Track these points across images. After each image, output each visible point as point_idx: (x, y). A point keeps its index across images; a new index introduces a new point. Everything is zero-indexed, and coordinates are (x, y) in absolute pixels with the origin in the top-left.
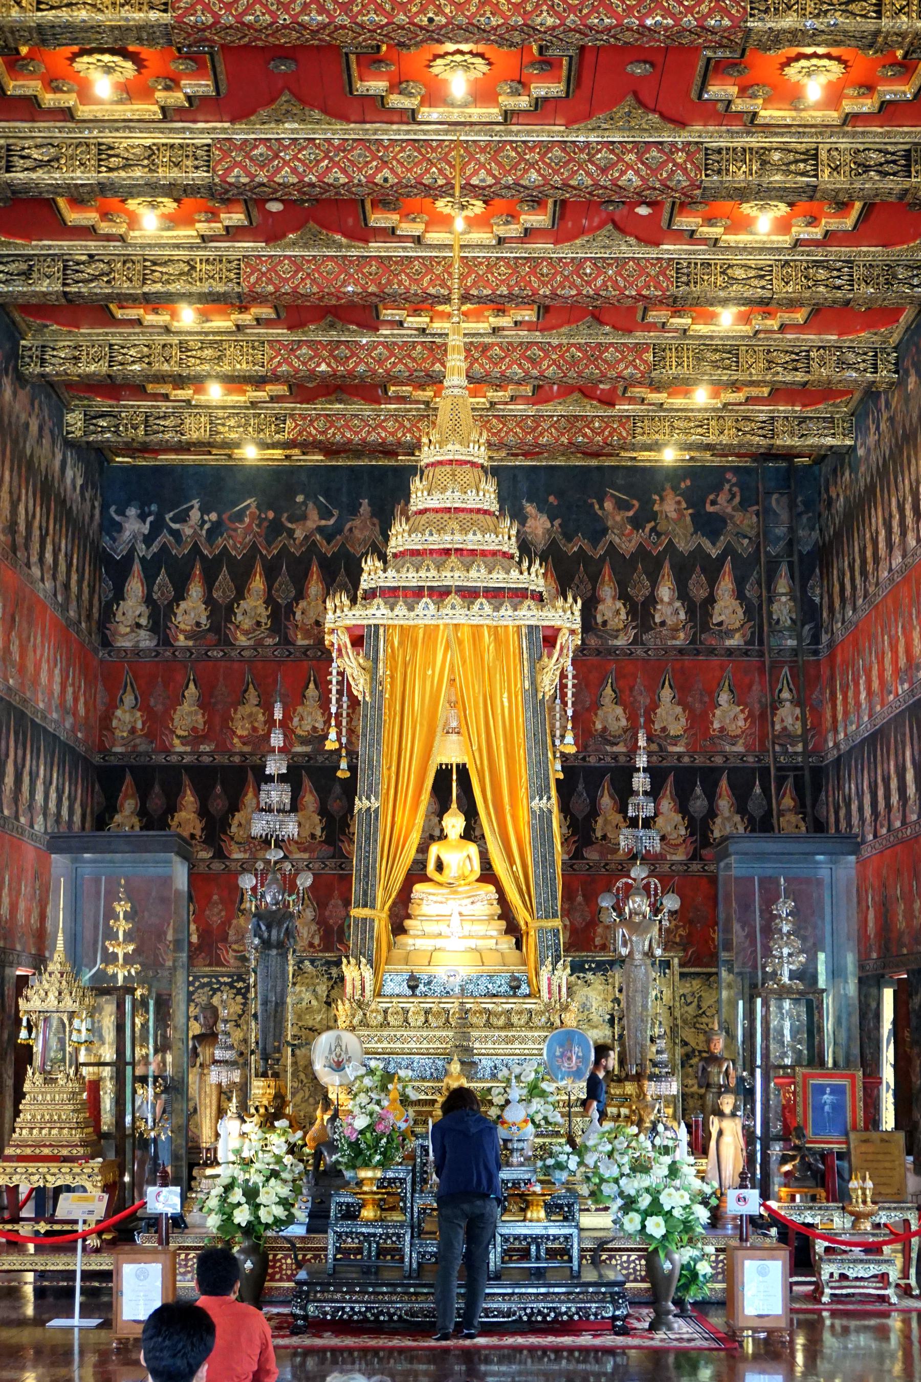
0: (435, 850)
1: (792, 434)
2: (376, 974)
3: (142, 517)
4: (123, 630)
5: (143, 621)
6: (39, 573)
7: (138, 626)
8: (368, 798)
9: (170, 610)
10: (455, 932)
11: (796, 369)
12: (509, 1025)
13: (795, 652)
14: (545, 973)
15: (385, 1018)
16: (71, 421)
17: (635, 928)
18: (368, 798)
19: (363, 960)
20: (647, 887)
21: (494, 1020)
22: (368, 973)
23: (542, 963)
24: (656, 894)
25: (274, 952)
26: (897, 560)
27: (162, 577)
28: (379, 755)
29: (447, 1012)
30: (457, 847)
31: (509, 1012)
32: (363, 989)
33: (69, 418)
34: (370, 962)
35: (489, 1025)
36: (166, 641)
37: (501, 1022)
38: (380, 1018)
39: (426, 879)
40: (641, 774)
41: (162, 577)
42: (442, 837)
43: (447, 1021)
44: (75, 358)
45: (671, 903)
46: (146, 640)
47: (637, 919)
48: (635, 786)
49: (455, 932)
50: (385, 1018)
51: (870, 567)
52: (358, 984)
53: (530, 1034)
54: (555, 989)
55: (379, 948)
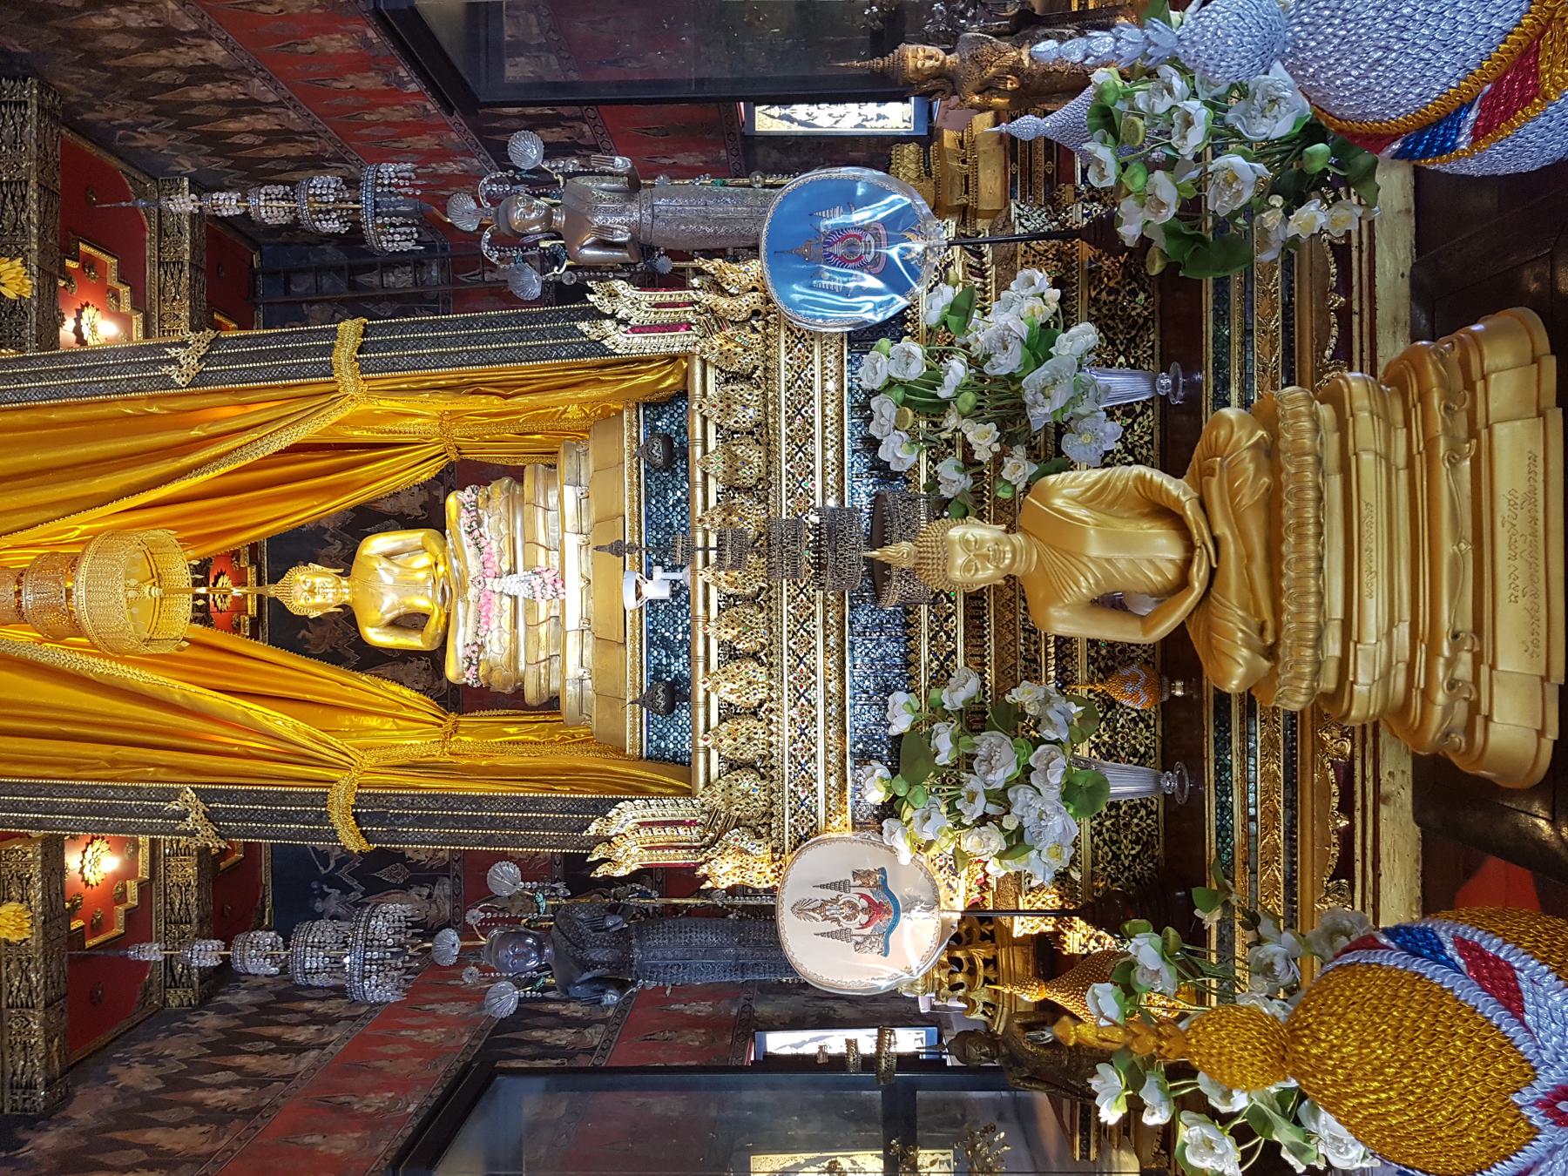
0: (377, 637)
1: (179, 243)
2: (638, 790)
3: (324, 896)
4: (434, 911)
5: (426, 892)
6: (313, 1054)
7: (430, 896)
8: (183, 816)
9: (414, 866)
10: (531, 585)
11: (24, 197)
12: (761, 433)
13: (442, 267)
14: (620, 341)
15: (751, 765)
16: (177, 1002)
17: (578, 221)
18: (183, 816)
19: (593, 829)
20: (494, 200)
21: (748, 475)
22: (627, 814)
23: (597, 347)
24: (514, 182)
25: (637, 954)
26: (258, 88)
27: (383, 875)
28: (66, 791)
29: (729, 601)
30: (365, 582)
31: (728, 436)
32: (675, 824)
33: (174, 1003)
34: (601, 808)
35: (760, 490)
36: (444, 870)
37: (756, 456)
38: (747, 782)
39: (435, 658)
40: (252, 202)
41: (383, 875)
42: (347, 617)
43: (752, 600)
44: (24, 1048)
45: (528, 150)
46: (444, 889)
47: (560, 219)
48: (285, 220)
49: (531, 585)
50: (751, 765)
51: (307, 150)
52: (662, 836)
53: (784, 375)
54: (666, 316)
55: (572, 775)
